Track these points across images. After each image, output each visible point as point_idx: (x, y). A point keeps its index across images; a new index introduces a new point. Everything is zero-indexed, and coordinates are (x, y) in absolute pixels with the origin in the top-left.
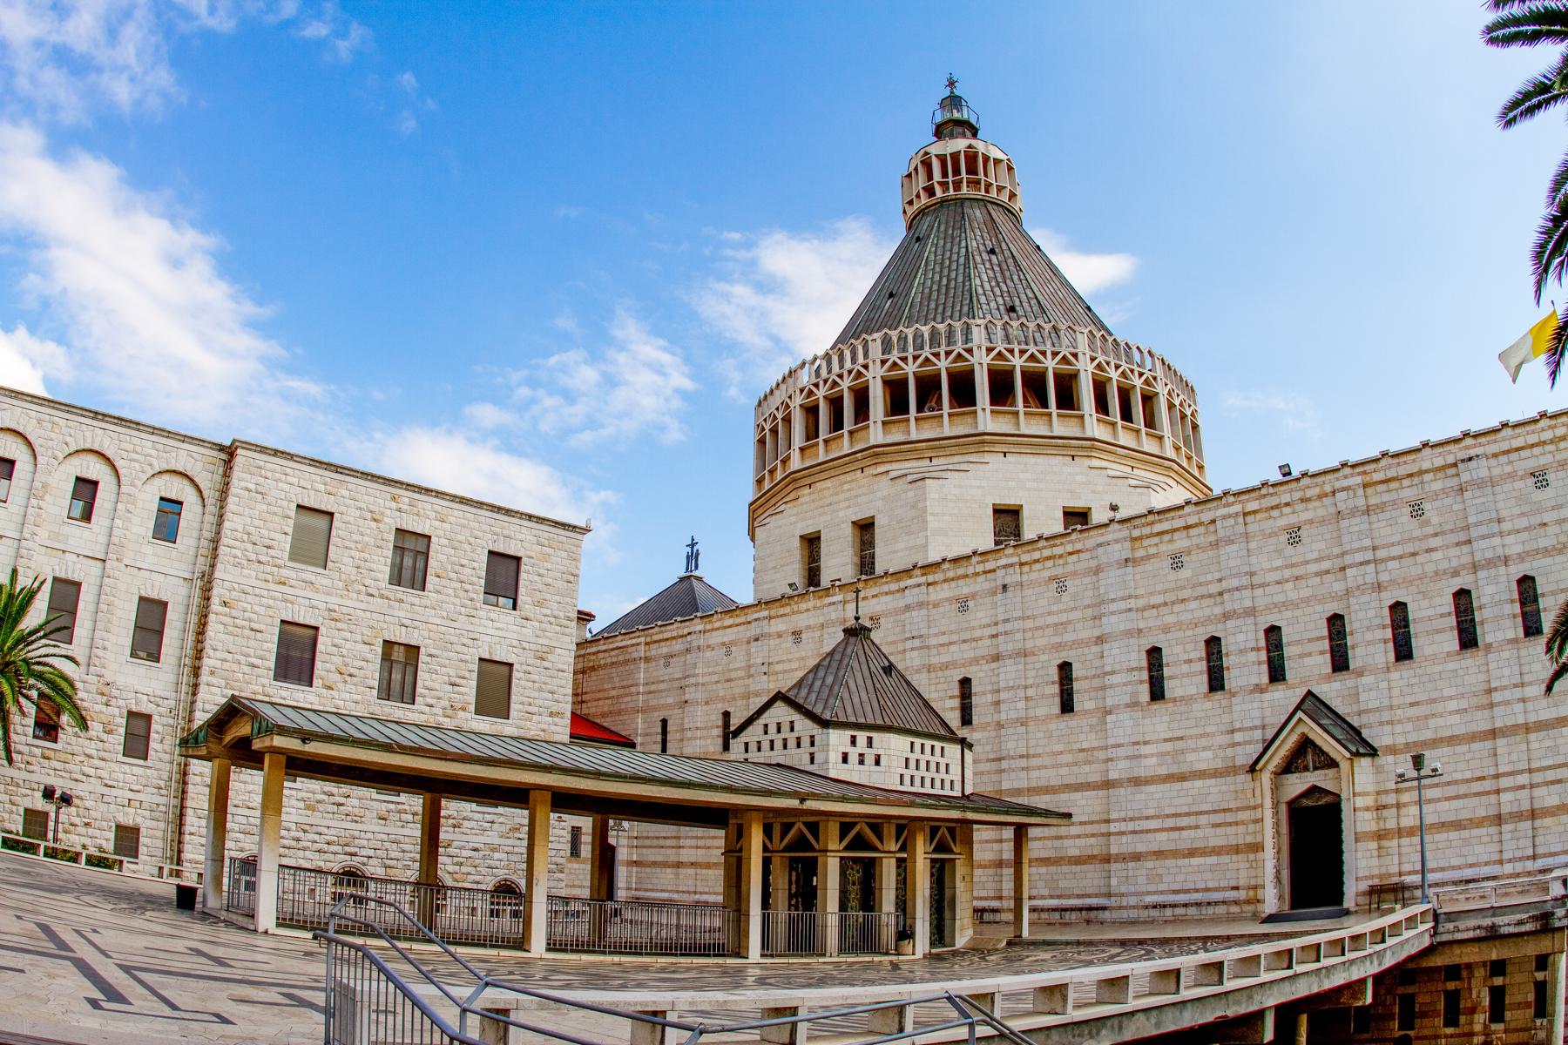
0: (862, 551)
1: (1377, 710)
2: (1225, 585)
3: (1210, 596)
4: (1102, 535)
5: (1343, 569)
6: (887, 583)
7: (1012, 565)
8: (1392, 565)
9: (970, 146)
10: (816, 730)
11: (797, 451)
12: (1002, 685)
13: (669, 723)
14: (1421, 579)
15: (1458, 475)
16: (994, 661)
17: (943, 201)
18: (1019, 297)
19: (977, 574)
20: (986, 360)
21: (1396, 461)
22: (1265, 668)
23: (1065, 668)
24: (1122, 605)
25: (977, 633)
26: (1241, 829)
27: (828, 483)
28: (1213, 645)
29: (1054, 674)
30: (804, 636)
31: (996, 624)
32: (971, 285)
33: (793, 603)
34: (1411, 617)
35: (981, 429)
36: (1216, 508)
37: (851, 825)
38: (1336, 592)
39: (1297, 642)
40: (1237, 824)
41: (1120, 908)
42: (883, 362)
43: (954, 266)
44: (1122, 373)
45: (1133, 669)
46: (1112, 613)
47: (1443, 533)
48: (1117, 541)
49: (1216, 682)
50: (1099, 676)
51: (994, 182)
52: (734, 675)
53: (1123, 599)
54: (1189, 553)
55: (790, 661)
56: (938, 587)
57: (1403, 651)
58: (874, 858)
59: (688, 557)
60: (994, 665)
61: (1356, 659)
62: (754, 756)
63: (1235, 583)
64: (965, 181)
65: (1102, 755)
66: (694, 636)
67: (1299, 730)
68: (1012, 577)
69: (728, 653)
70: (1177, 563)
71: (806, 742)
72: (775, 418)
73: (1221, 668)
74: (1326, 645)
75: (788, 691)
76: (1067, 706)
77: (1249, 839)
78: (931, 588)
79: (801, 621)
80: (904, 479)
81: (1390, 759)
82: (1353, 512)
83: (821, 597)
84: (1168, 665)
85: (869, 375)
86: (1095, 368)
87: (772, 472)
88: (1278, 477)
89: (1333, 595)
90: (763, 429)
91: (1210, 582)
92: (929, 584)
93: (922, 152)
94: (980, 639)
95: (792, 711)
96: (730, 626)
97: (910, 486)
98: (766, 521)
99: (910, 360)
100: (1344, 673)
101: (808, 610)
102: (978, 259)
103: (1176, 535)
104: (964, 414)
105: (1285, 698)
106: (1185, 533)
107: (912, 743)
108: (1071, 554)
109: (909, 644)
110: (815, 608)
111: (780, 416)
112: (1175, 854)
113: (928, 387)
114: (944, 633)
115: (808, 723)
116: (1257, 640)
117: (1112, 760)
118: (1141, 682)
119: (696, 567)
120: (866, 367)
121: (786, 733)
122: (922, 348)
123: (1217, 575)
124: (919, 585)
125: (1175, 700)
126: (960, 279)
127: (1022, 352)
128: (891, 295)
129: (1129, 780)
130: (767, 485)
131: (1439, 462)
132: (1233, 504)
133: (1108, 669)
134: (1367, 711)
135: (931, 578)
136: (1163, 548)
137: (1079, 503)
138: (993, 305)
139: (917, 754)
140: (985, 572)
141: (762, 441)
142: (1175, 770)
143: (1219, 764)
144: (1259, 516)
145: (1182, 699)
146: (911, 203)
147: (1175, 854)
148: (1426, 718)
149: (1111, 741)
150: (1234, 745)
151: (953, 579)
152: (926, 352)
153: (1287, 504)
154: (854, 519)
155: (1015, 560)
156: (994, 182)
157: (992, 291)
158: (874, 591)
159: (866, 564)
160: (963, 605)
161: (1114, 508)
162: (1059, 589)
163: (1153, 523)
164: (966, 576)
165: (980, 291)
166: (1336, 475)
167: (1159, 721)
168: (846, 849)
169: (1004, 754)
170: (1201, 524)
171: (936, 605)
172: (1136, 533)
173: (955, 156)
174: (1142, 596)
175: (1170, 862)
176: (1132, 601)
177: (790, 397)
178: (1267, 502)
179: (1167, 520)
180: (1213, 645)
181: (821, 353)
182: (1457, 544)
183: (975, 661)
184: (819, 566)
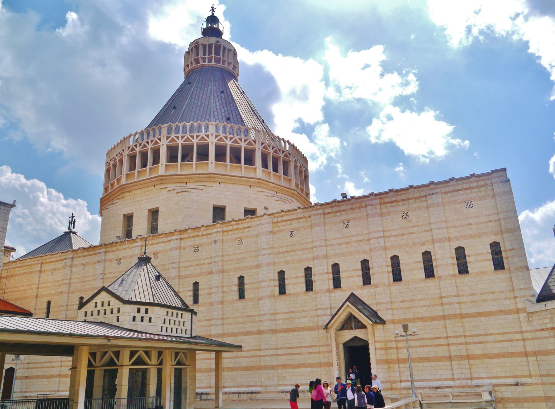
0: (152, 223)
1: (385, 303)
2: (314, 244)
3: (307, 249)
4: (260, 220)
5: (369, 240)
6: (162, 238)
7: (219, 232)
8: (392, 239)
9: (217, 42)
10: (120, 305)
11: (125, 175)
12: (213, 285)
13: (52, 303)
14: (406, 246)
15: (427, 201)
16: (209, 275)
17: (202, 67)
18: (232, 114)
19: (203, 235)
20: (215, 141)
21: (396, 193)
22: (331, 282)
23: (241, 279)
24: (268, 251)
25: (202, 262)
26: (322, 355)
27: (138, 191)
28: (308, 271)
29: (236, 282)
30: (122, 261)
31: (211, 258)
32: (211, 106)
33: (117, 245)
34: (401, 262)
35: (210, 171)
36: (312, 211)
37: (136, 352)
38: (365, 250)
39: (346, 271)
40: (319, 353)
41: (267, 392)
42: (168, 138)
43: (204, 97)
44: (275, 150)
45: (271, 280)
46: (264, 255)
47: (418, 226)
48: (267, 223)
49: (309, 286)
50: (256, 283)
51: (227, 60)
52: (86, 279)
53: (268, 249)
54: (298, 230)
55: (115, 272)
56: (186, 240)
57: (397, 276)
58: (147, 368)
59: (70, 223)
60: (210, 276)
61: (374, 279)
62: (89, 318)
63: (319, 243)
64: (214, 58)
65: (257, 319)
66: (67, 260)
67: (348, 310)
68: (219, 237)
69: (84, 269)
70: (293, 234)
71: (115, 311)
72: (115, 159)
73: (311, 281)
74: (360, 273)
75: (108, 287)
76: (242, 296)
77: (326, 360)
78: (182, 241)
79: (121, 254)
80: (174, 191)
81: (392, 326)
83: (131, 243)
84: (287, 279)
85: (161, 143)
86: (263, 148)
87: (112, 185)
88: (340, 198)
89: (364, 251)
90: (110, 164)
91: (308, 243)
92: (181, 239)
93: (195, 42)
94: (204, 264)
95: (109, 296)
96: (86, 256)
97: (176, 195)
98: (108, 207)
99: (180, 138)
100: (369, 286)
101: (124, 249)
102: (215, 95)
103: (293, 222)
104: (203, 164)
106: (297, 221)
107: (167, 312)
108: (246, 228)
109: (171, 266)
110: (128, 248)
111: (118, 159)
112: (291, 366)
114: (187, 261)
115: (117, 302)
116: (328, 269)
117: (261, 321)
118: (275, 286)
119: (74, 227)
120: (160, 139)
122: (186, 133)
123: (311, 240)
124: (177, 239)
125: (290, 295)
126: (207, 103)
127: (231, 139)
128: (174, 108)
129: (270, 331)
130: (109, 191)
131: (417, 195)
132: (319, 209)
133: (260, 279)
134: (381, 303)
135: (182, 236)
136: (287, 227)
137: (251, 206)
138: (220, 116)
139: (169, 317)
140: (207, 235)
141: (108, 171)
142: (290, 326)
143: (311, 325)
144: (330, 215)
145: (293, 294)
146: (188, 66)
147: (291, 366)
148: (409, 308)
149: (262, 313)
150: (318, 316)
151: (193, 237)
153: (344, 210)
154: (149, 208)
155: (221, 229)
156: (227, 60)
157: (220, 110)
158: (156, 241)
159: (154, 229)
160: (196, 249)
161: (266, 209)
162: (240, 243)
163: (283, 216)
164: (198, 236)
165: (215, 109)
166: (367, 199)
167: (283, 303)
168: (133, 364)
169: (213, 317)
170: (304, 217)
172: (275, 220)
173: (210, 46)
174: (276, 248)
175: (289, 370)
176: (272, 249)
177: (123, 150)
178: (335, 209)
179: (289, 215)
180: (308, 271)
181: (139, 131)
182: (425, 231)
183: (200, 274)
184: (132, 229)
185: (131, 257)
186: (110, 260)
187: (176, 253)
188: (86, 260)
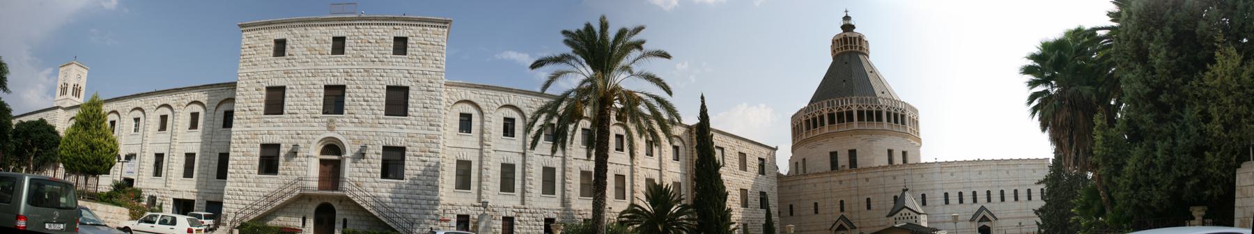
20: (886, 109)
28: (960, 194)
30: (843, 182)
49: (961, 201)
57: (1003, 199)
68: (909, 172)
69: (815, 186)
70: (952, 175)
79: (842, 178)
82: (994, 170)
85: (853, 109)
105: (977, 207)
113: (870, 113)
120: (852, 106)
121: (908, 215)
152: (870, 105)
167: (948, 208)
171: (886, 177)
185: (850, 180)
186: (835, 181)
187: (881, 179)
188: (816, 181)
